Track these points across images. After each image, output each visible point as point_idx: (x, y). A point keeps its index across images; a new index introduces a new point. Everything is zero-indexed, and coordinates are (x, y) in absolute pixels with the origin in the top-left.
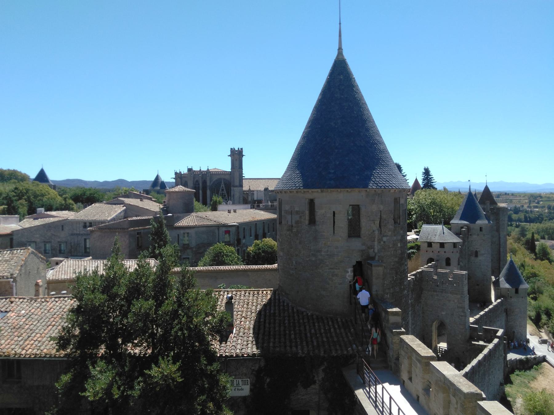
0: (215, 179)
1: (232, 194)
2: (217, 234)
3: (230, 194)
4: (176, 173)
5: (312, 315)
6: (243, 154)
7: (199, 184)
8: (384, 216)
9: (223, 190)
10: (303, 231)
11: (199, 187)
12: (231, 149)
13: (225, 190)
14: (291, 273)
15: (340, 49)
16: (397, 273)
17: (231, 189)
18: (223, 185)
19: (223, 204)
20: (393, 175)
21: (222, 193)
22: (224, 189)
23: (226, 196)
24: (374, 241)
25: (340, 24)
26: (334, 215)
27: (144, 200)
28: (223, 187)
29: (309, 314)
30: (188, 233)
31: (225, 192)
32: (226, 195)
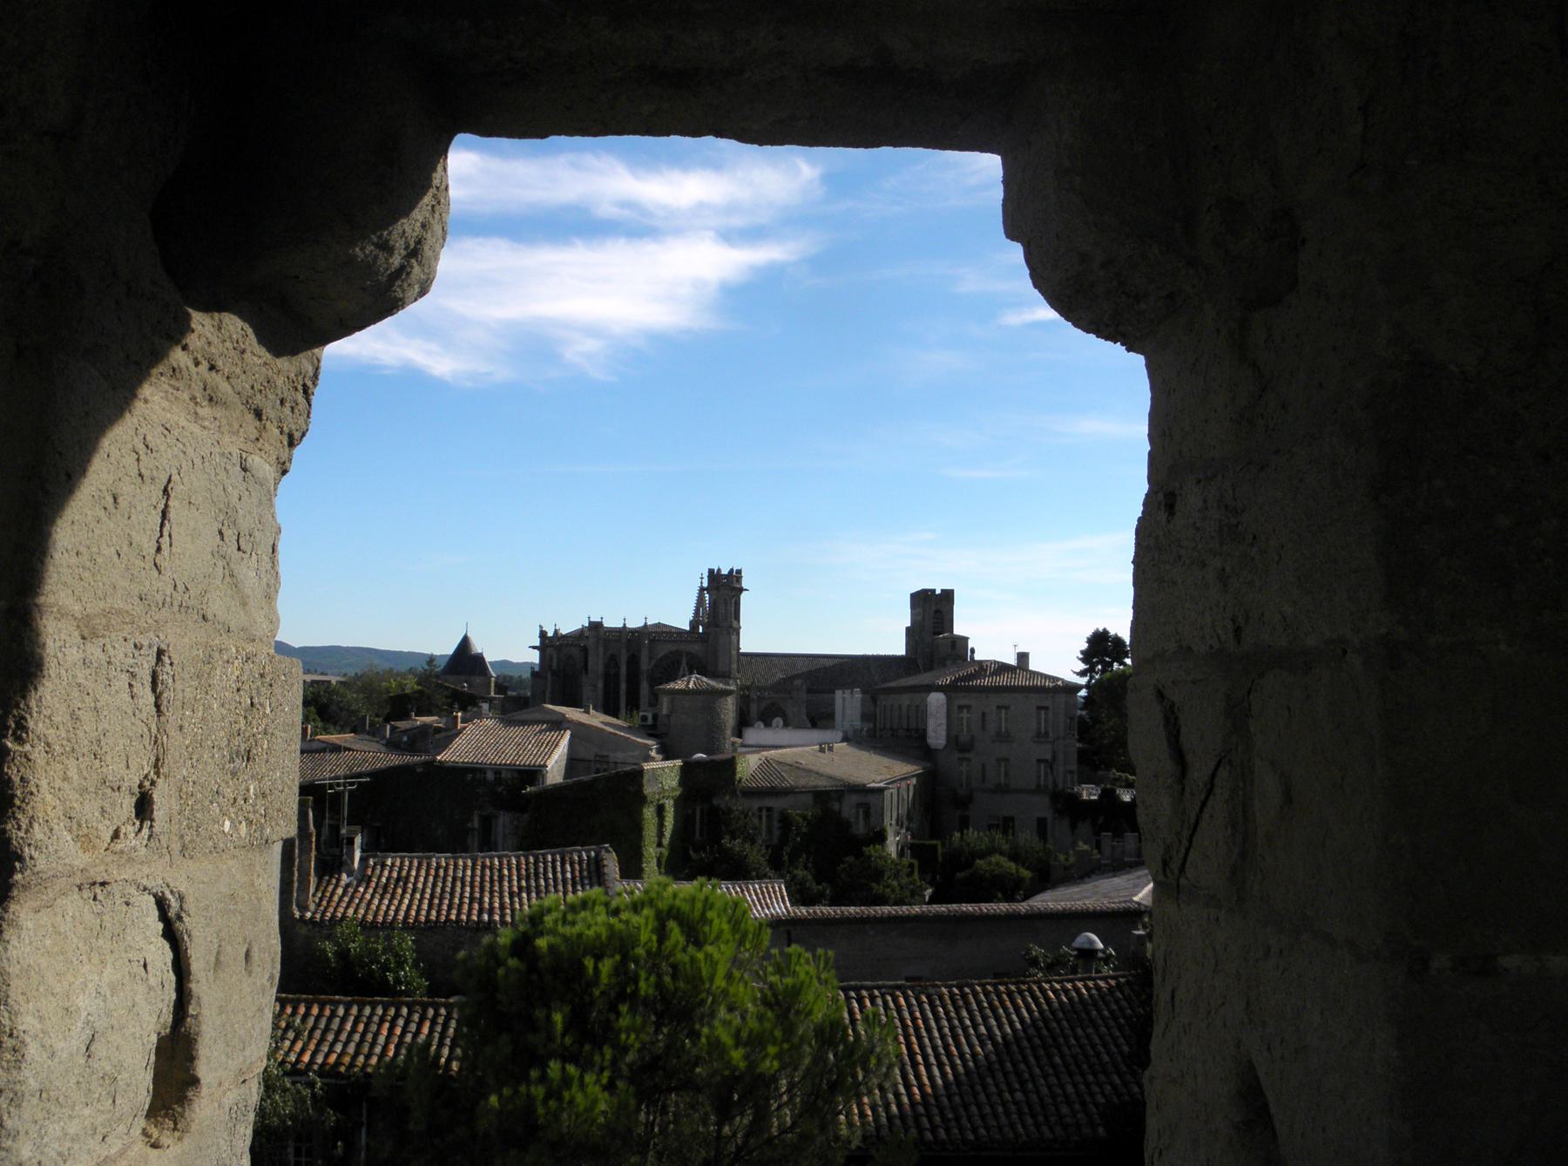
0: (662, 651)
4: (543, 634)
6: (744, 584)
7: (617, 666)
11: (617, 675)
12: (711, 571)
19: (759, 727)
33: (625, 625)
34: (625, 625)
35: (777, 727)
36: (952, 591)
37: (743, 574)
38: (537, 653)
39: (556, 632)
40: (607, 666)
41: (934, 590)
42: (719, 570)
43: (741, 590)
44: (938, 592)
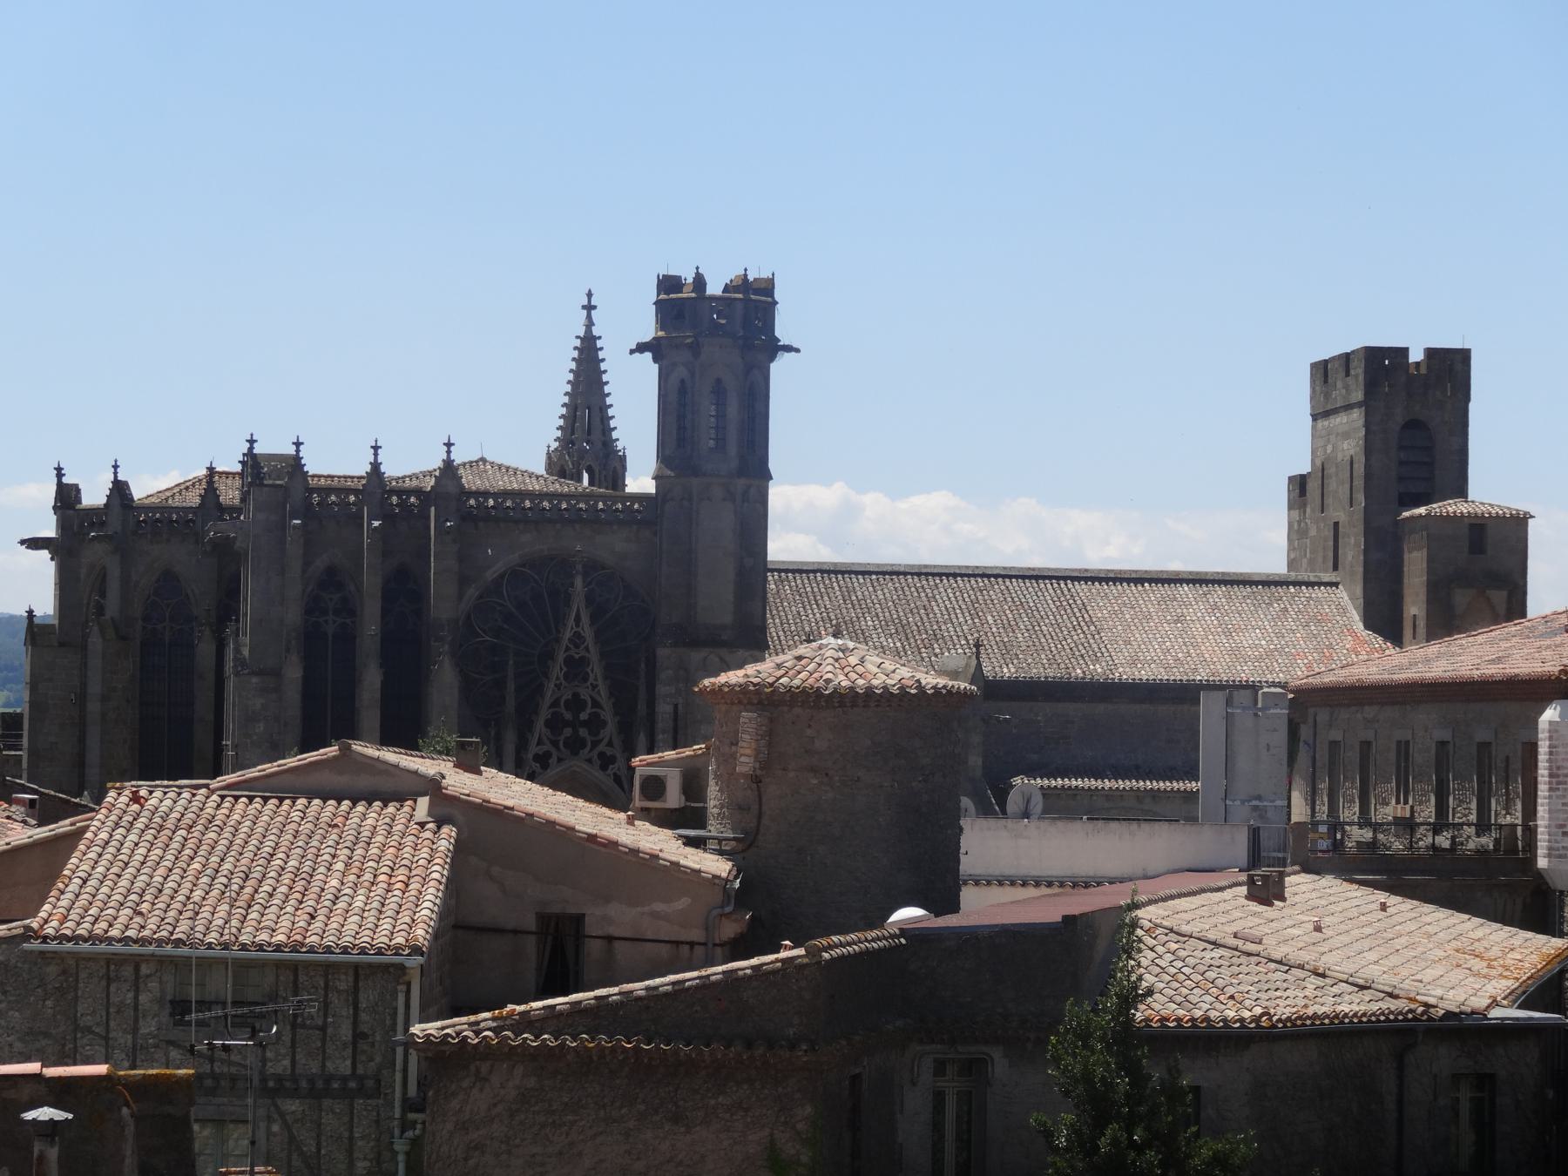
0: (498, 557)
3: (642, 708)
4: (66, 497)
6: (784, 330)
11: (347, 638)
12: (668, 284)
13: (596, 670)
17: (652, 663)
18: (578, 623)
21: (568, 695)
22: (594, 655)
23: (610, 730)
28: (577, 639)
31: (597, 687)
32: (608, 715)
33: (376, 466)
34: (376, 466)
36: (1463, 356)
37: (778, 296)
38: (43, 566)
39: (120, 489)
40: (313, 607)
41: (1403, 352)
42: (700, 282)
43: (774, 348)
44: (1416, 356)
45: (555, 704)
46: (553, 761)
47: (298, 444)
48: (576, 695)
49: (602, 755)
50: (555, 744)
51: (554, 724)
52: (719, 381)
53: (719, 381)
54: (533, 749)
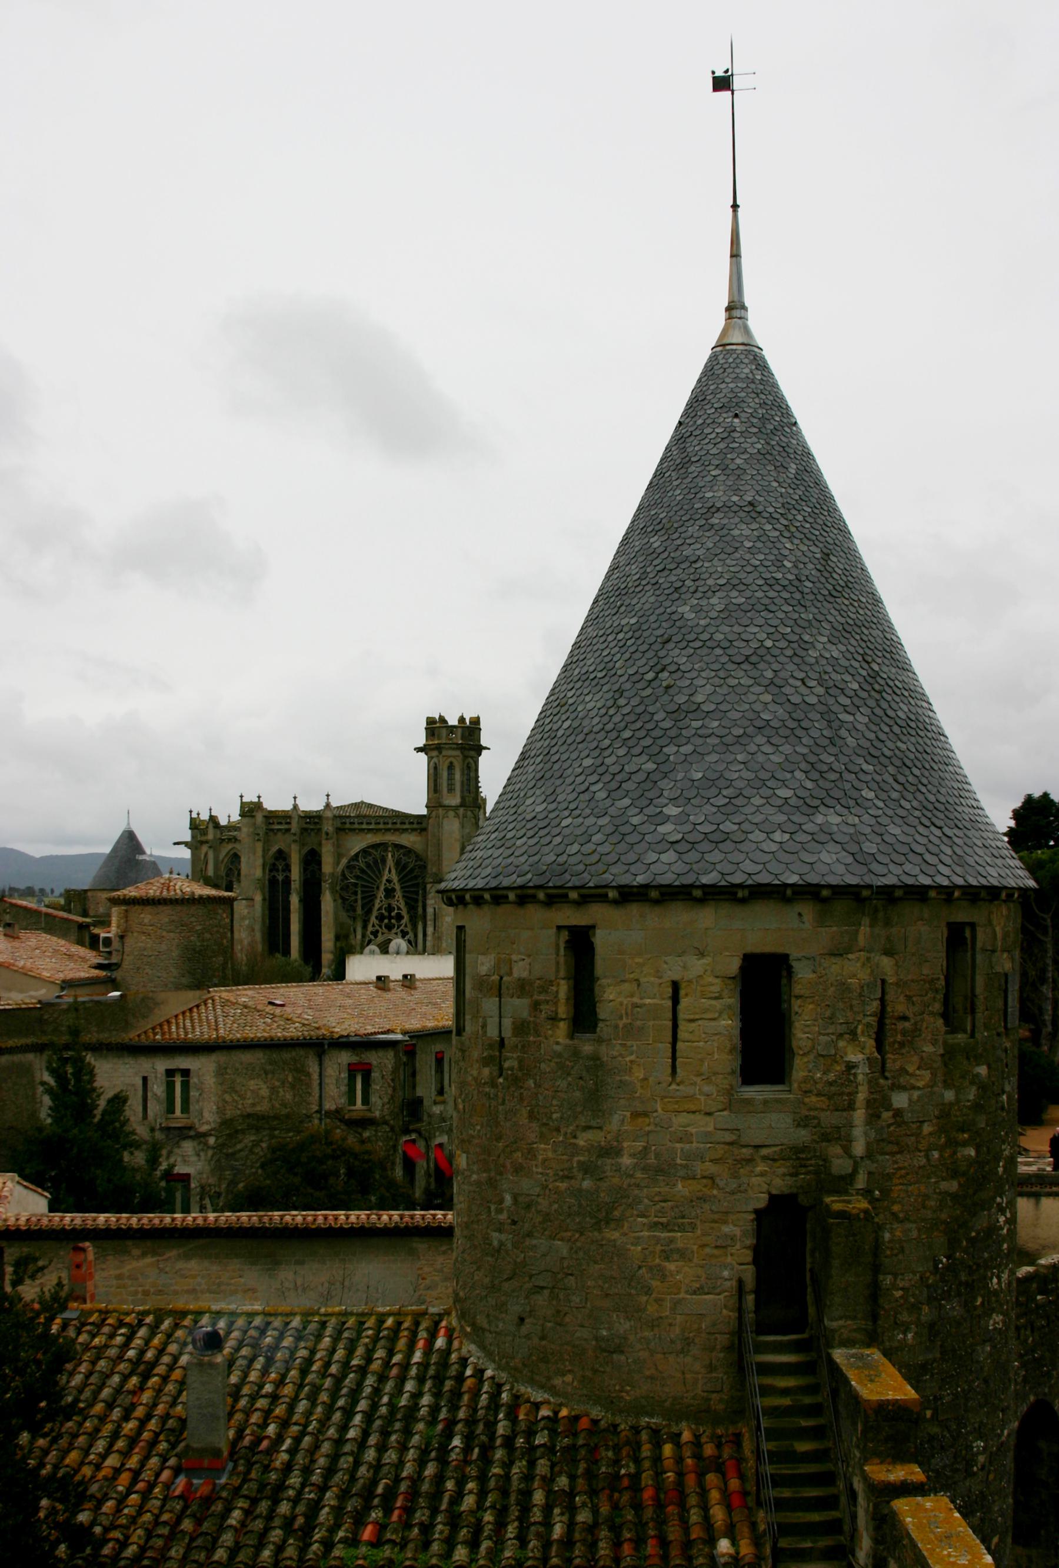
0: (356, 844)
1: (430, 911)
2: (316, 1076)
3: (420, 910)
4: (195, 825)
5: (575, 1419)
7: (288, 868)
8: (898, 1005)
9: (389, 893)
10: (543, 1066)
11: (287, 881)
12: (430, 721)
13: (399, 894)
14: (495, 1243)
15: (735, 308)
16: (953, 1244)
17: (424, 889)
18: (390, 874)
19: (372, 953)
20: (946, 830)
22: (397, 887)
23: (406, 919)
24: (851, 1107)
25: (735, 206)
26: (675, 1000)
27: (22, 934)
29: (564, 1412)
30: (186, 1073)
31: (399, 901)
32: (404, 913)
33: (295, 807)
34: (295, 807)
35: (398, 953)
40: (273, 868)
42: (442, 720)
45: (380, 909)
46: (380, 934)
47: (259, 797)
48: (389, 905)
49: (402, 931)
50: (380, 926)
51: (381, 918)
52: (451, 763)
53: (451, 763)
54: (370, 928)
